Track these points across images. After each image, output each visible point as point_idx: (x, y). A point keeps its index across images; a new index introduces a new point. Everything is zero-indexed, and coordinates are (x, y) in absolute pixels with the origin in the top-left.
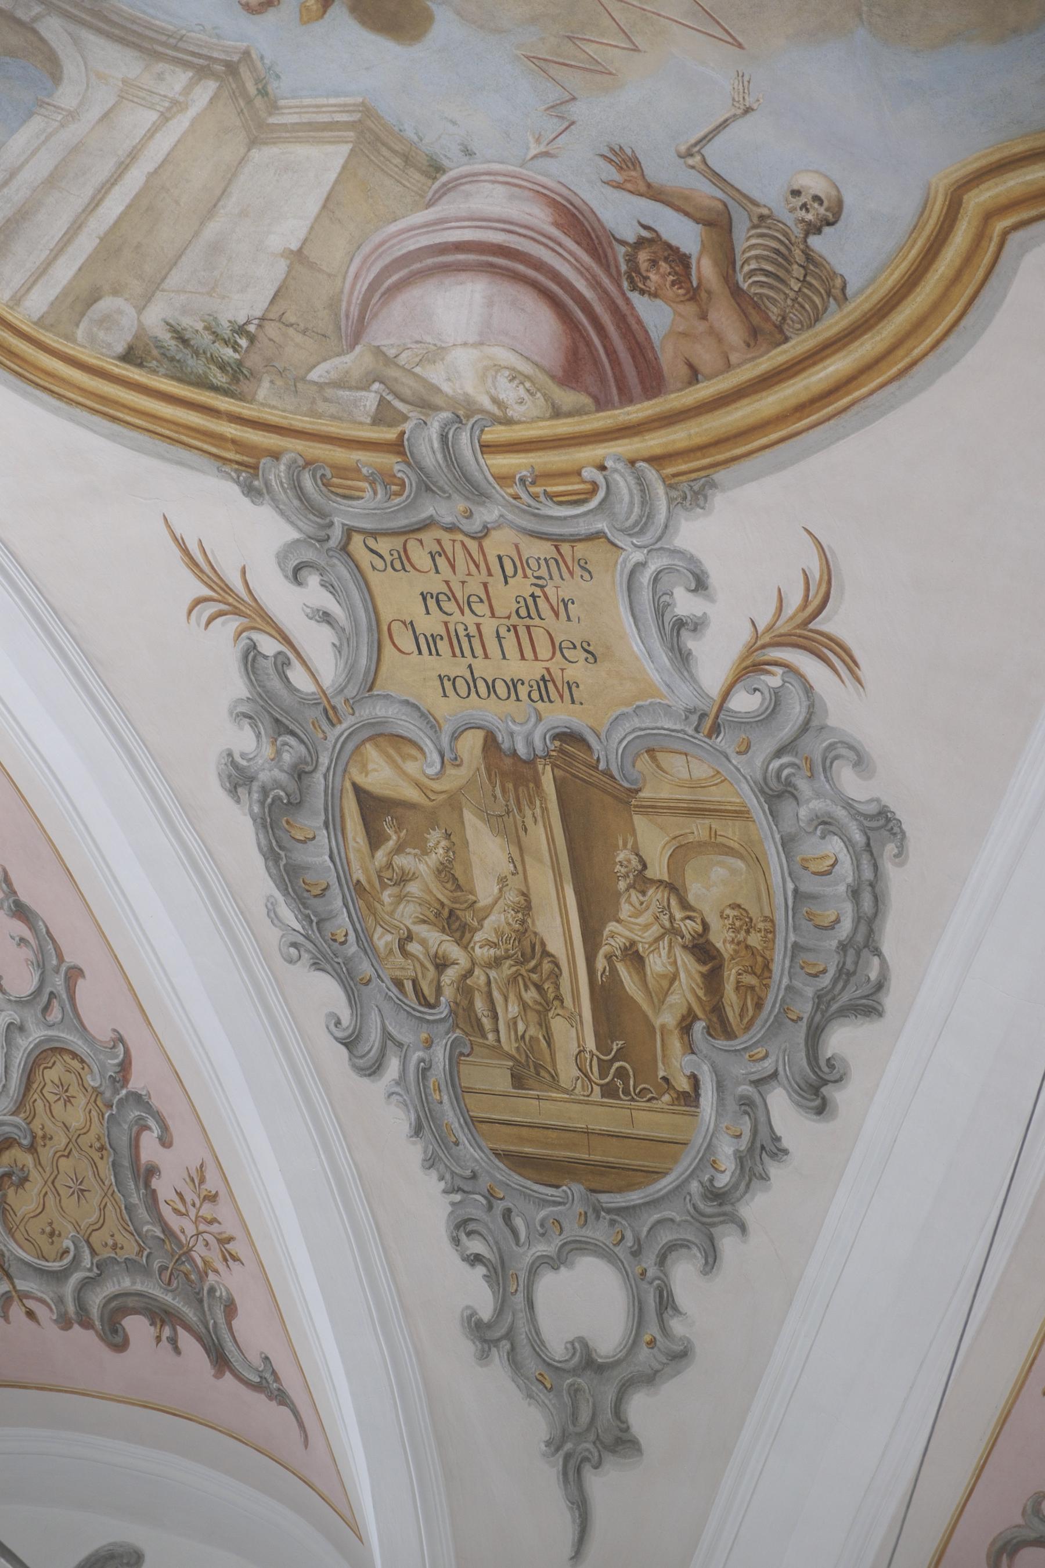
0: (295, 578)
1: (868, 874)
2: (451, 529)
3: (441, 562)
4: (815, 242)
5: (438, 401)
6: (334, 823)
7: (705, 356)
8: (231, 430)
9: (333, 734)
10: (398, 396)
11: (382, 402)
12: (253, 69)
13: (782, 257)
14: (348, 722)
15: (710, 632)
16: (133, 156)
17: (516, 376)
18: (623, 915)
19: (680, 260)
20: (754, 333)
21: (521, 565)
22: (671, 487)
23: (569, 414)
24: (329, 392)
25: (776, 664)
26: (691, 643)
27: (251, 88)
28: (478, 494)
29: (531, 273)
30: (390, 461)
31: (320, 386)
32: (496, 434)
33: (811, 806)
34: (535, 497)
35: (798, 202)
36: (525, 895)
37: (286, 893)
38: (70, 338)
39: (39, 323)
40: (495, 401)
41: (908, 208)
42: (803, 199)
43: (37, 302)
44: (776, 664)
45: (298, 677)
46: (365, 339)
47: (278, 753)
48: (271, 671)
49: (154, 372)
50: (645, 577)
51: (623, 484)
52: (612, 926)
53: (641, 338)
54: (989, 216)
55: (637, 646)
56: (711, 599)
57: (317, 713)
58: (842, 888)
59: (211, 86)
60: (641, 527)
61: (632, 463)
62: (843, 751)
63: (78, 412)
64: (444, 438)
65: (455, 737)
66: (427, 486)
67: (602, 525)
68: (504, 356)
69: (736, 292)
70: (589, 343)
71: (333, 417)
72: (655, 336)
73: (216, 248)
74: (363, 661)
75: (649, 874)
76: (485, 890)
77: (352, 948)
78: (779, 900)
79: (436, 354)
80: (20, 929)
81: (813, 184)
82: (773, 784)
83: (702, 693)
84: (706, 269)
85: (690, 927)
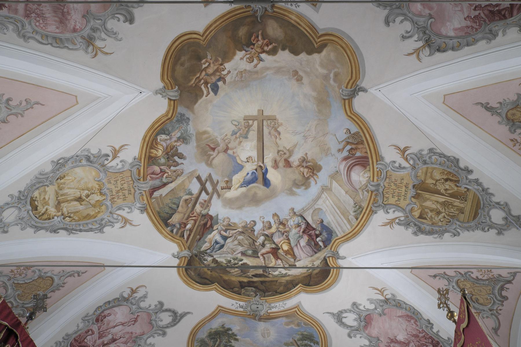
0: (387, 212)
1: (438, 154)
2: (384, 190)
3: (388, 193)
4: (352, 133)
5: (367, 184)
6: (423, 223)
7: (364, 150)
8: (367, 212)
9: (410, 218)
10: (365, 189)
11: (366, 191)
12: (323, 187)
13: (353, 137)
14: (408, 215)
15: (401, 163)
16: (332, 206)
17: (364, 173)
18: (440, 189)
19: (352, 149)
20: (362, 144)
21: (389, 183)
22: (381, 161)
23: (370, 169)
24: (364, 197)
25: (407, 156)
26: (402, 166)
27: (325, 188)
28: (379, 185)
29: (351, 166)
30: (374, 193)
31: (363, 198)
32: (371, 179)
33: (427, 158)
34: (380, 178)
35: (347, 133)
36: (436, 201)
37: (432, 235)
38: (354, 225)
39: (351, 228)
40: (367, 177)
41: (349, 122)
42: (346, 132)
43: (349, 227)
44: (407, 156)
45: (402, 219)
46: (358, 189)
47: (412, 226)
48: (401, 222)
49: (359, 217)
50: (393, 169)
51: (379, 166)
52: (441, 191)
53: (361, 157)
54: (351, 113)
55: (402, 173)
56: (397, 161)
57: (407, 219)
58: (440, 158)
59: (324, 192)
60: (386, 166)
61: (377, 164)
62: (420, 152)
63: (363, 229)
64: (371, 186)
65: (412, 202)
66: (378, 191)
67: (385, 171)
68: (361, 174)
69: (357, 144)
70: (361, 163)
71: (367, 197)
72: (361, 155)
73: (344, 202)
74: (400, 209)
75: (434, 183)
76: (434, 206)
77: (441, 229)
78: (440, 167)
79: (360, 182)
80: (438, 278)
81: (345, 131)
82: (424, 162)
83: (410, 167)
84: (353, 146)
85: (443, 181)
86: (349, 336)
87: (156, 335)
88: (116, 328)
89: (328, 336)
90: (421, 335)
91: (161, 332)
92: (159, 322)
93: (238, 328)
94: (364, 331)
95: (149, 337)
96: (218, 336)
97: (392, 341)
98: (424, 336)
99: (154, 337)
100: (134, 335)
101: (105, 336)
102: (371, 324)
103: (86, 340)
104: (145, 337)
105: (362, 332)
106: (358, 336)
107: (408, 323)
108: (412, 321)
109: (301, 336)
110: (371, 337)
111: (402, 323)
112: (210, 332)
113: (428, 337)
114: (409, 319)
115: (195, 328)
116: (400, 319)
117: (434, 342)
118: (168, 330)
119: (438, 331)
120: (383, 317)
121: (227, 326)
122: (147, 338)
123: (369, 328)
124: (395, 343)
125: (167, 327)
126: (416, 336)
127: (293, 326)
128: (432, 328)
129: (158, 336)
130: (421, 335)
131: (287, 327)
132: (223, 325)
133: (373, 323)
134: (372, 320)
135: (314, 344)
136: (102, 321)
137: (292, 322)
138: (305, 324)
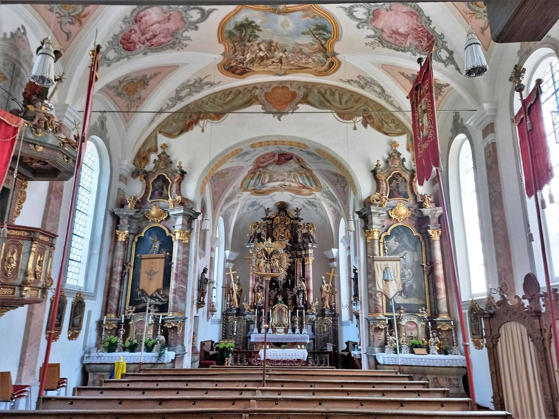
86: (358, 27)
87: (189, 30)
88: (154, 26)
89: (339, 27)
90: (420, 29)
91: (193, 27)
92: (190, 19)
93: (261, 21)
94: (371, 24)
95: (184, 31)
96: (243, 28)
97: (394, 32)
98: (422, 30)
99: (188, 31)
100: (171, 31)
101: (146, 33)
102: (378, 18)
103: (131, 38)
104: (181, 32)
105: (370, 24)
106: (366, 27)
107: (410, 19)
108: (415, 17)
109: (316, 27)
110: (377, 28)
111: (405, 18)
112: (236, 25)
113: (425, 31)
114: (412, 15)
115: (222, 22)
116: (404, 15)
117: (429, 36)
118: (199, 25)
119: (435, 27)
120: (390, 12)
121: (250, 19)
122: (183, 33)
123: (376, 21)
124: (397, 34)
125: (198, 22)
126: (415, 30)
127: (309, 18)
128: (430, 24)
129: (191, 30)
130: (420, 29)
131: (303, 19)
132: (247, 19)
133: (380, 17)
134: (380, 14)
135: (327, 33)
136: (140, 21)
137: (308, 15)
138: (319, 16)
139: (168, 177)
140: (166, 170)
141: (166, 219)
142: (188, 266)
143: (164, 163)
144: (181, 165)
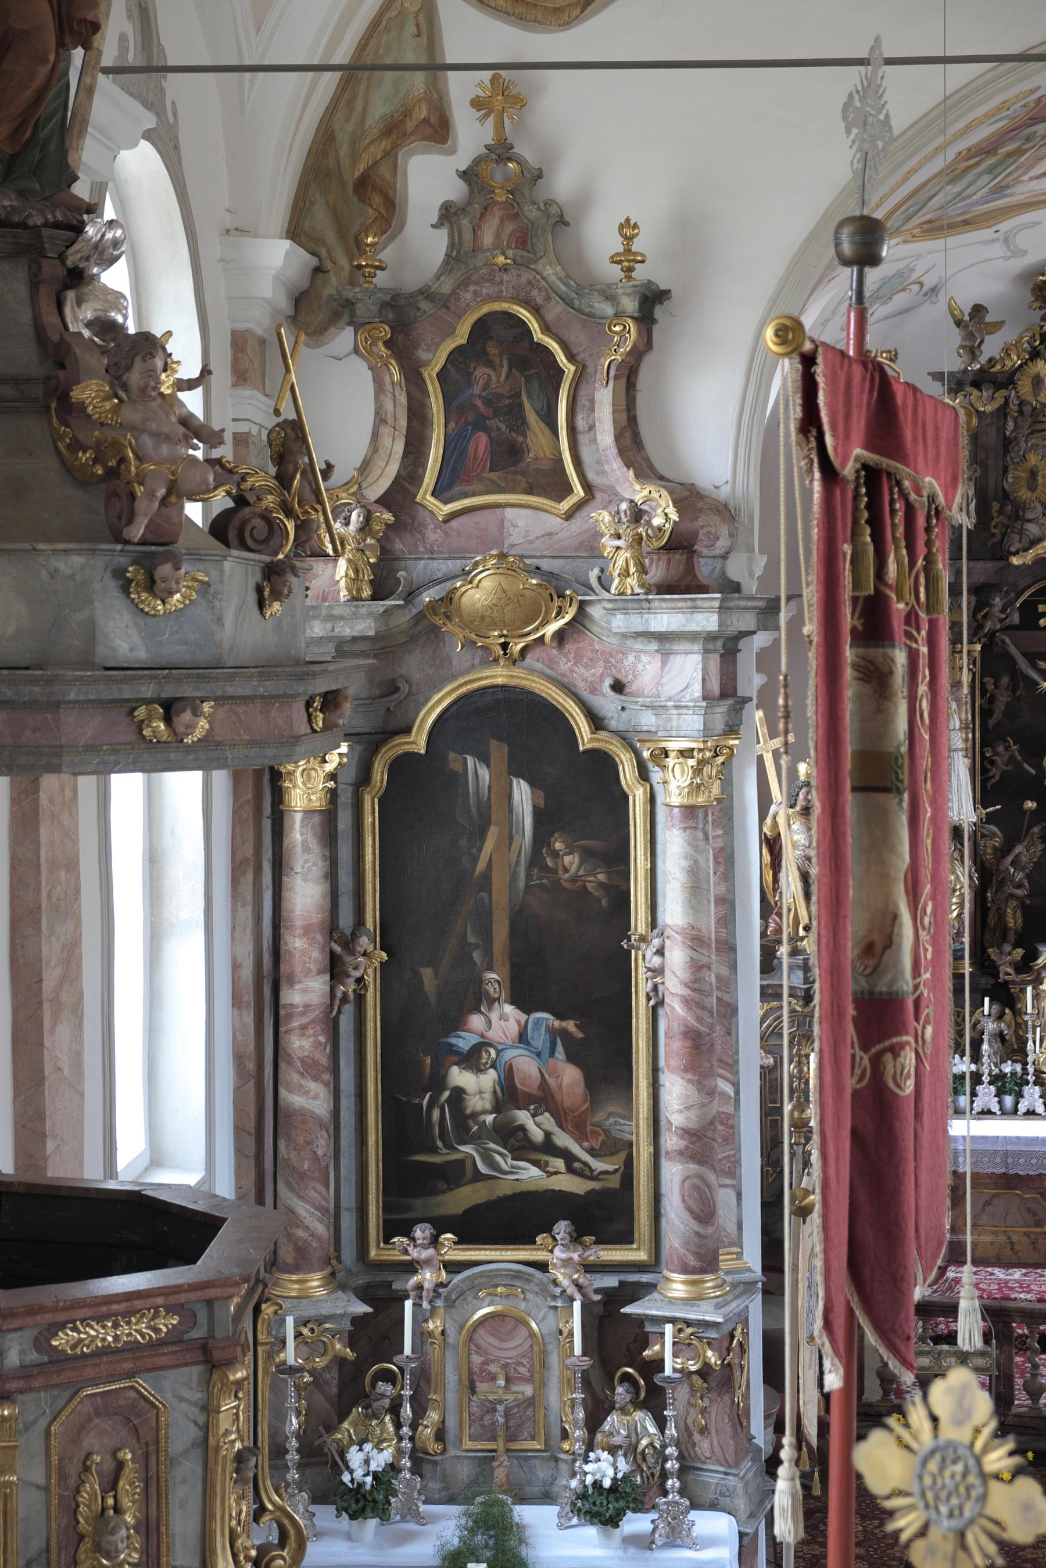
139: (546, 329)
140: (526, 276)
141: (560, 636)
142: (733, 949)
143: (510, 227)
144: (637, 246)
